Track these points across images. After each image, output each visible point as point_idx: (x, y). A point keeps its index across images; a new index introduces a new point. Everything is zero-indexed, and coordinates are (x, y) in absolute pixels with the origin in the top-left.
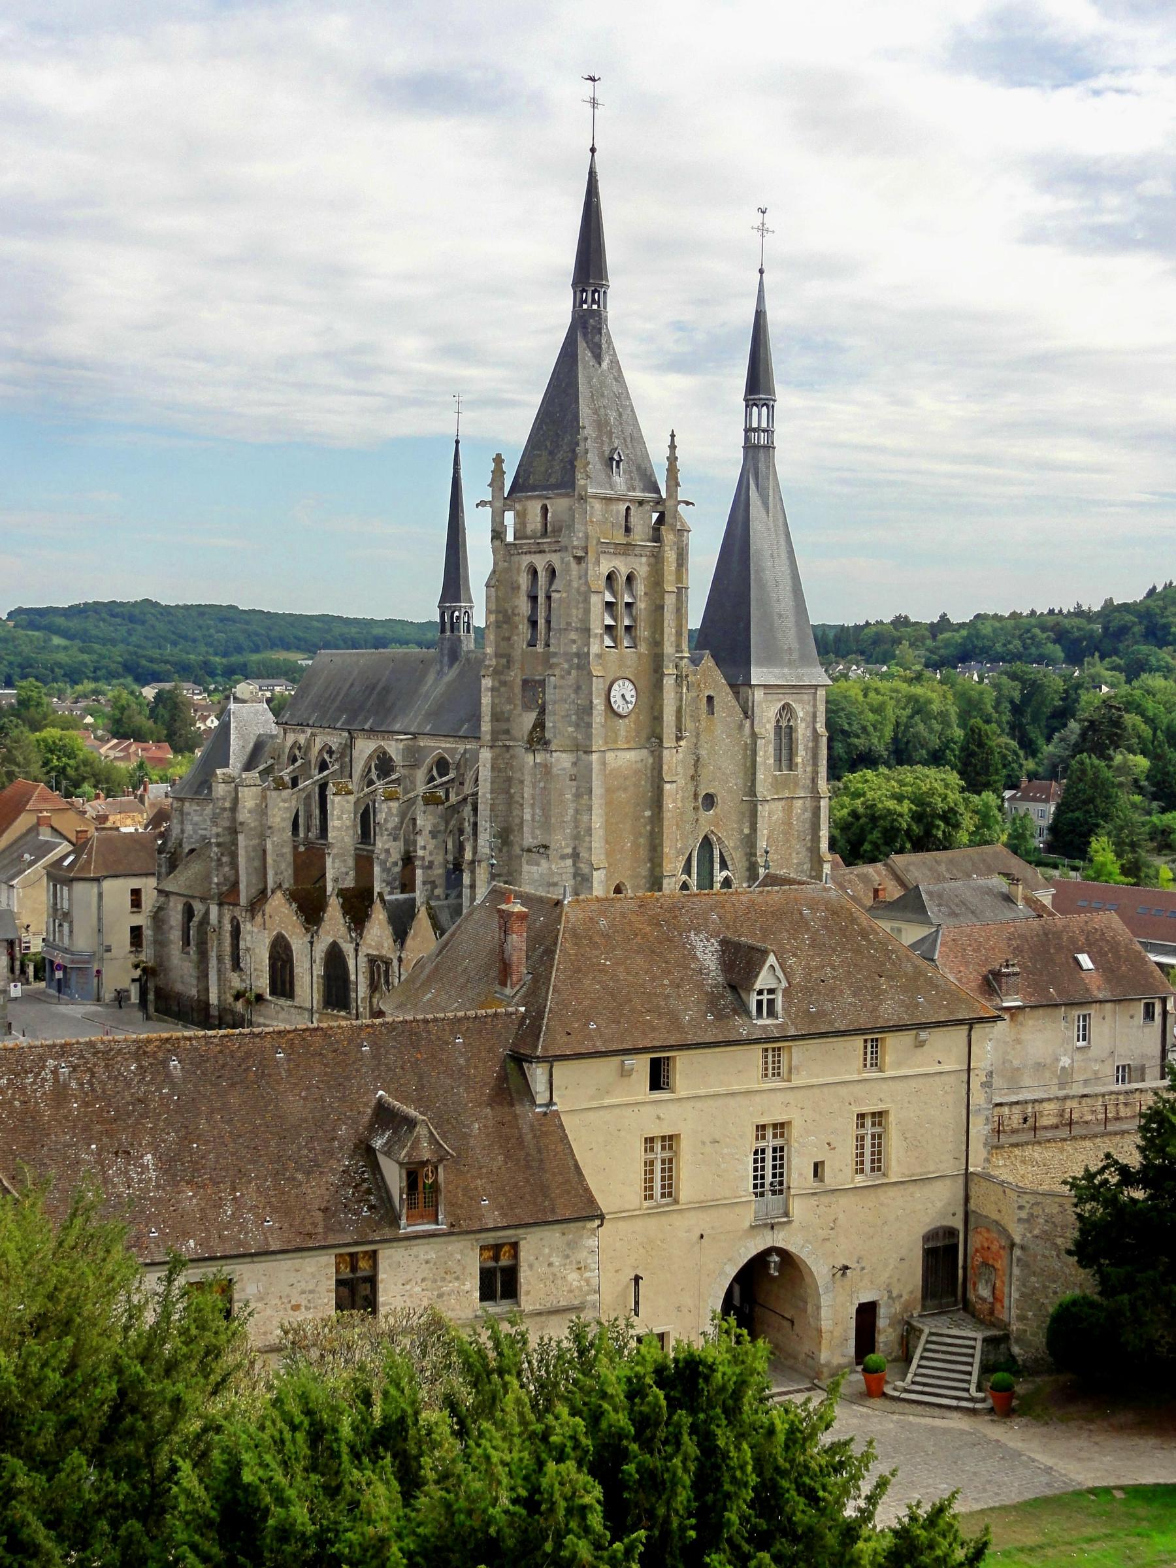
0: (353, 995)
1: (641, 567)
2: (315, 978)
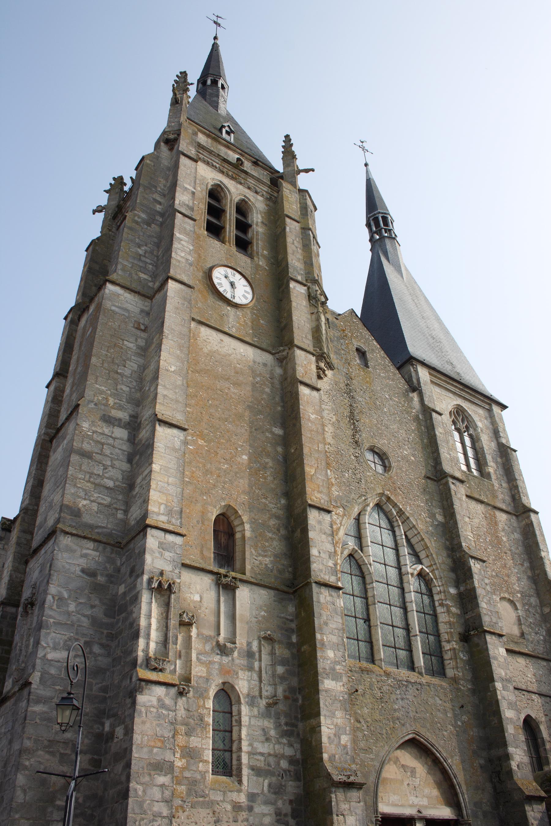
1: (258, 205)
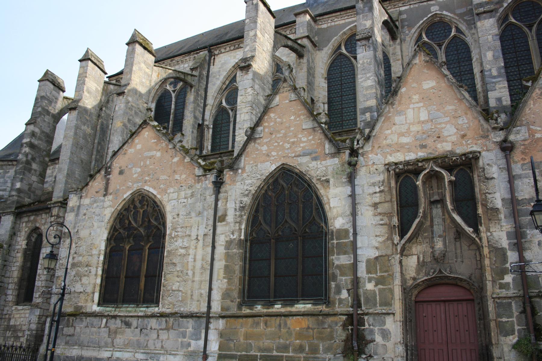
0: (342, 260)
2: (220, 250)
